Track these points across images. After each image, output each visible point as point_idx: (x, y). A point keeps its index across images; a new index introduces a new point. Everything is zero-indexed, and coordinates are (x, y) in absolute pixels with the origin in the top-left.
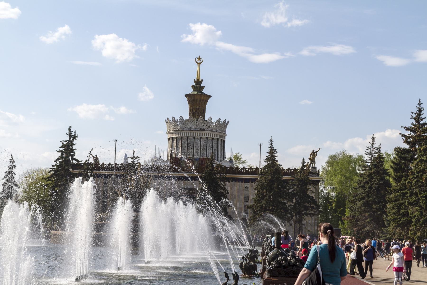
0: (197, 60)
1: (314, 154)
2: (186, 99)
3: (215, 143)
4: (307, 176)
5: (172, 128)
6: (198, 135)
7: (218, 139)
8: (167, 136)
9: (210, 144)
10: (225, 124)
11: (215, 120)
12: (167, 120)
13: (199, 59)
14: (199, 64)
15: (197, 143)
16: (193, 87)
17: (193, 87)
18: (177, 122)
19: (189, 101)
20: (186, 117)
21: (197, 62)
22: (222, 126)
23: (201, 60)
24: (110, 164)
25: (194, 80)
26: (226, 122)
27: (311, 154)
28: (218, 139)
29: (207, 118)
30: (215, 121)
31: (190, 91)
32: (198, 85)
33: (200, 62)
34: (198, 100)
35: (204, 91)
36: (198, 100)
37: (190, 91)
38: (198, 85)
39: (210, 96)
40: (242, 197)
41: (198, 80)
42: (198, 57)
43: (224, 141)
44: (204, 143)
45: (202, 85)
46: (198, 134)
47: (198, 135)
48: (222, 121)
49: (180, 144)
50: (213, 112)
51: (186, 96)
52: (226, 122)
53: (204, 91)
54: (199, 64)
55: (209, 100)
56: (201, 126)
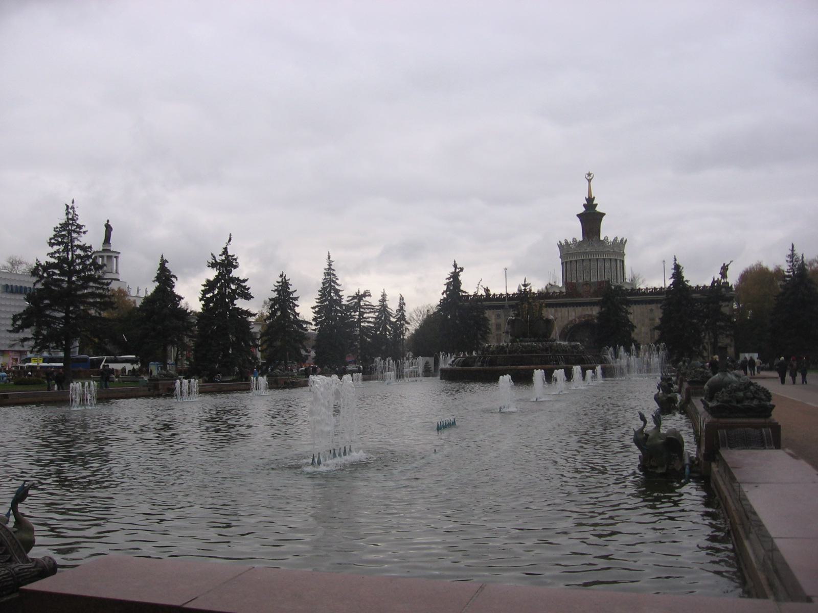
0: (587, 176)
3: (613, 263)
6: (594, 256)
7: (616, 260)
10: (623, 243)
11: (611, 239)
12: (559, 243)
13: (589, 175)
14: (589, 181)
16: (584, 205)
17: (584, 205)
18: (571, 244)
20: (580, 238)
21: (586, 178)
23: (592, 175)
24: (501, 295)
25: (586, 198)
26: (624, 240)
27: (722, 268)
28: (616, 260)
29: (602, 238)
30: (612, 240)
31: (582, 210)
32: (590, 204)
33: (590, 178)
35: (598, 209)
36: (591, 218)
37: (582, 210)
38: (590, 204)
39: (604, 214)
41: (589, 197)
42: (588, 173)
43: (623, 261)
45: (594, 203)
47: (594, 256)
48: (619, 239)
51: (578, 215)
52: (624, 240)
53: (598, 209)
54: (589, 181)
55: (604, 218)
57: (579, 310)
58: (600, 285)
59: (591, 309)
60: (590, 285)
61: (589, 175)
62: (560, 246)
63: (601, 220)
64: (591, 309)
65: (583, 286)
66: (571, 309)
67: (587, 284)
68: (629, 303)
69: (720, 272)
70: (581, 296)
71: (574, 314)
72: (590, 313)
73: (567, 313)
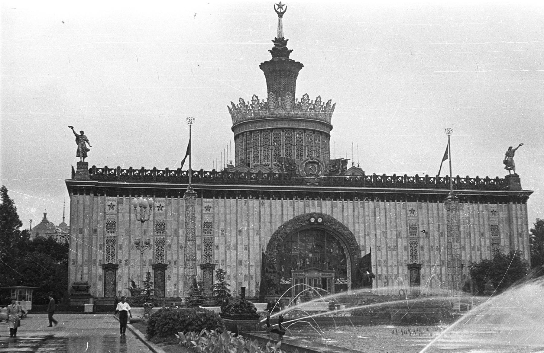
0: (277, 7)
12: (231, 106)
13: (280, 6)
14: (280, 15)
23: (284, 8)
31: (269, 57)
33: (282, 11)
37: (269, 57)
42: (278, 3)
54: (280, 15)
55: (300, 72)
58: (334, 166)
59: (320, 206)
60: (318, 164)
62: (234, 111)
63: (297, 74)
64: (320, 206)
65: (306, 164)
66: (287, 203)
67: (315, 162)
69: (504, 159)
71: (291, 210)
72: (318, 211)
73: (279, 209)
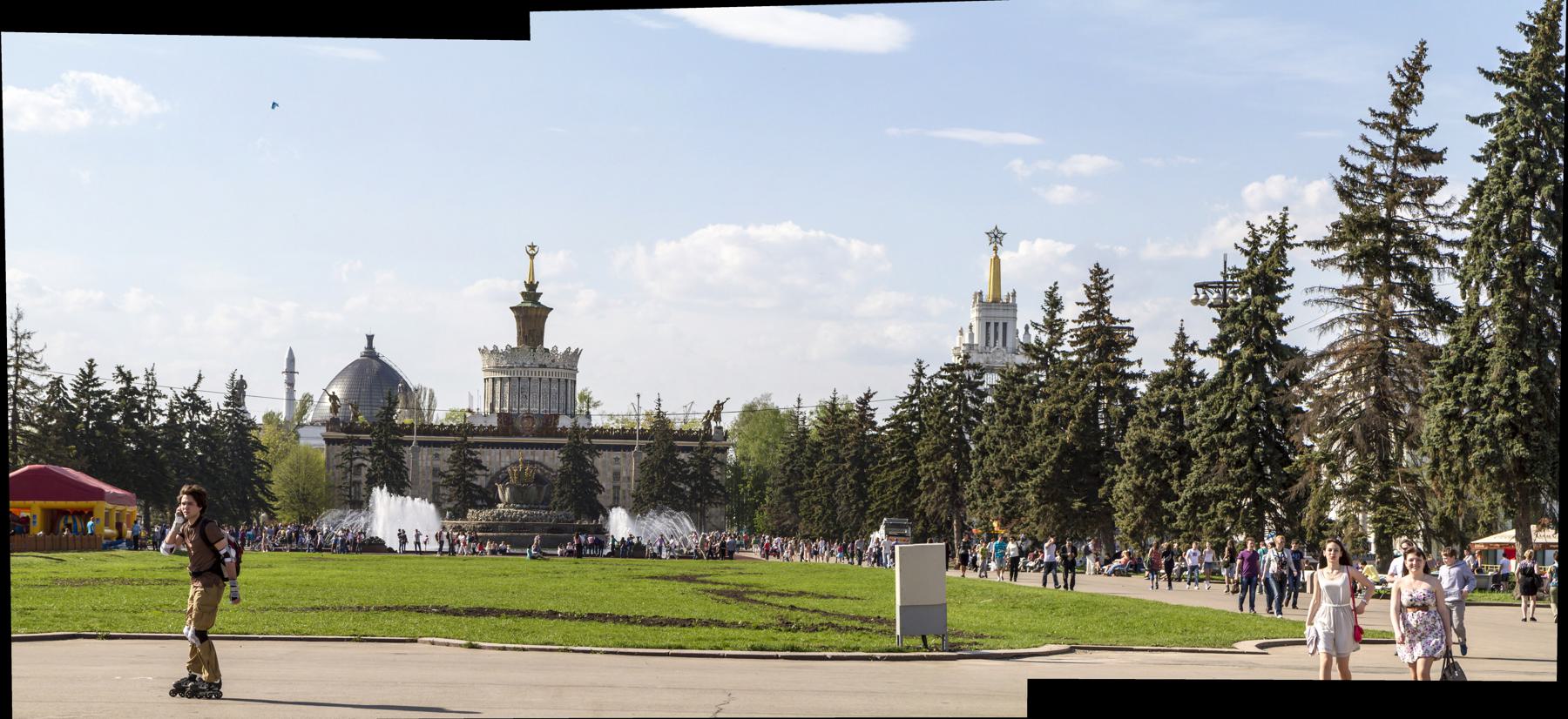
1: (719, 406)
2: (512, 315)
3: (563, 385)
4: (707, 441)
5: (493, 363)
8: (484, 375)
9: (555, 388)
13: (533, 247)
14: (532, 256)
15: (535, 386)
16: (523, 294)
17: (523, 294)
19: (517, 318)
20: (514, 345)
22: (573, 357)
32: (531, 292)
34: (531, 316)
36: (531, 316)
37: (519, 301)
38: (531, 292)
40: (610, 474)
44: (545, 386)
46: (536, 373)
49: (507, 388)
50: (555, 337)
53: (541, 300)
54: (532, 256)
56: (540, 361)
57: (518, 454)
61: (533, 247)
66: (504, 451)
68: (595, 450)
70: (518, 434)
